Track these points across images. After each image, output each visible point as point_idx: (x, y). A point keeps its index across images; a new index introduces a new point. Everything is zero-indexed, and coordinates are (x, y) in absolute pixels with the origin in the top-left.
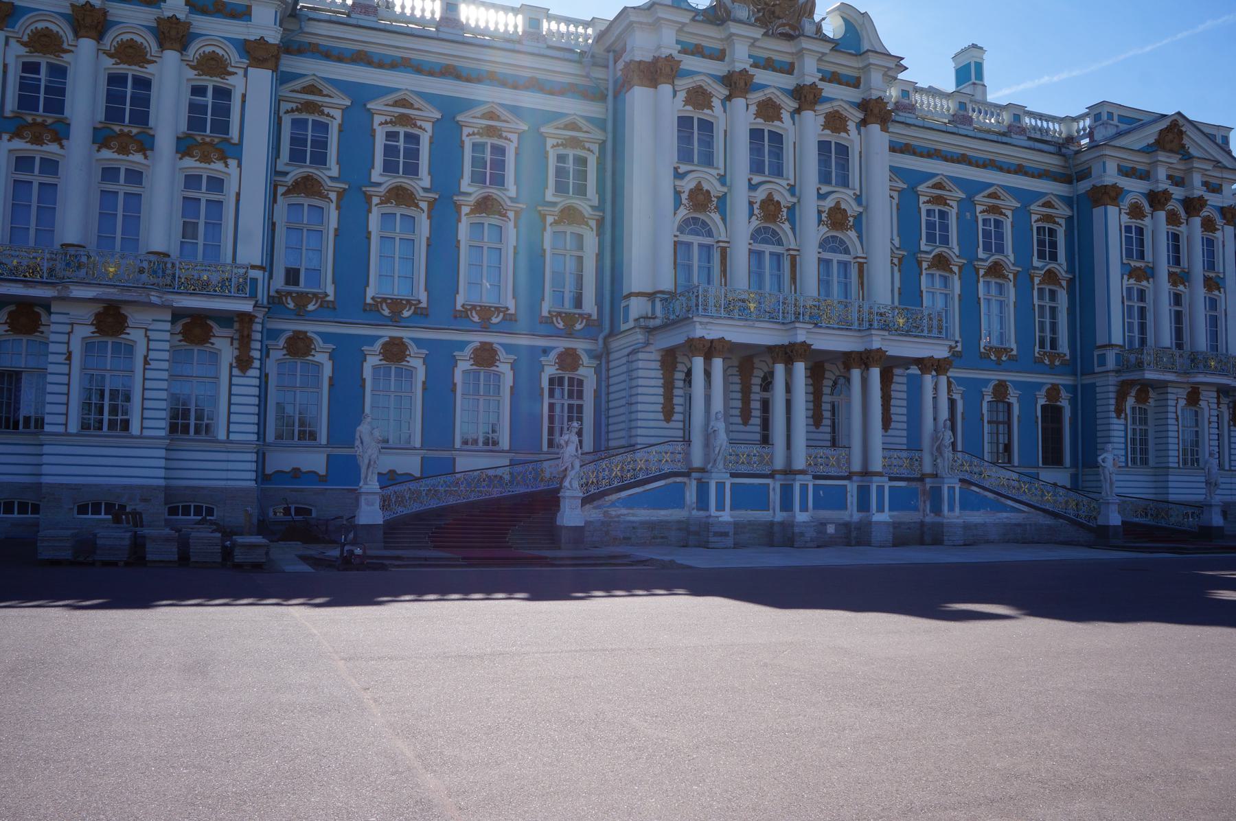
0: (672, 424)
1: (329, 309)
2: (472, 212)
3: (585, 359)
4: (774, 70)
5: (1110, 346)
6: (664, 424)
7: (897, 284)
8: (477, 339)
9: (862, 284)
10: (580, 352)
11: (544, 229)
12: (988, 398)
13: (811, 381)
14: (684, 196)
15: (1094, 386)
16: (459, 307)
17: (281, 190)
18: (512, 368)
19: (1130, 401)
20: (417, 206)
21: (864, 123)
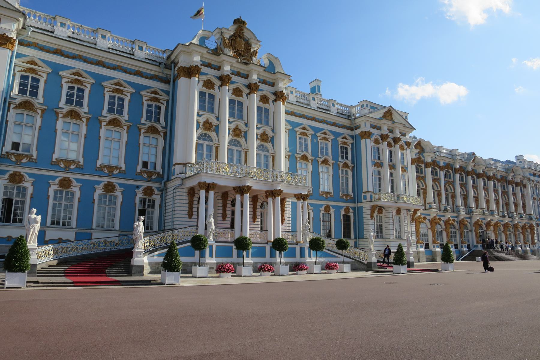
0: (191, 220)
1: (32, 162)
2: (107, 124)
3: (156, 191)
4: (240, 77)
5: (368, 192)
6: (188, 220)
7: (288, 166)
8: (106, 180)
9: (273, 164)
10: (153, 188)
11: (140, 135)
12: (323, 212)
13: (251, 203)
14: (201, 124)
15: (362, 207)
16: (98, 166)
17: (12, 106)
18: (122, 194)
19: (376, 213)
20: (81, 120)
21: (275, 101)
